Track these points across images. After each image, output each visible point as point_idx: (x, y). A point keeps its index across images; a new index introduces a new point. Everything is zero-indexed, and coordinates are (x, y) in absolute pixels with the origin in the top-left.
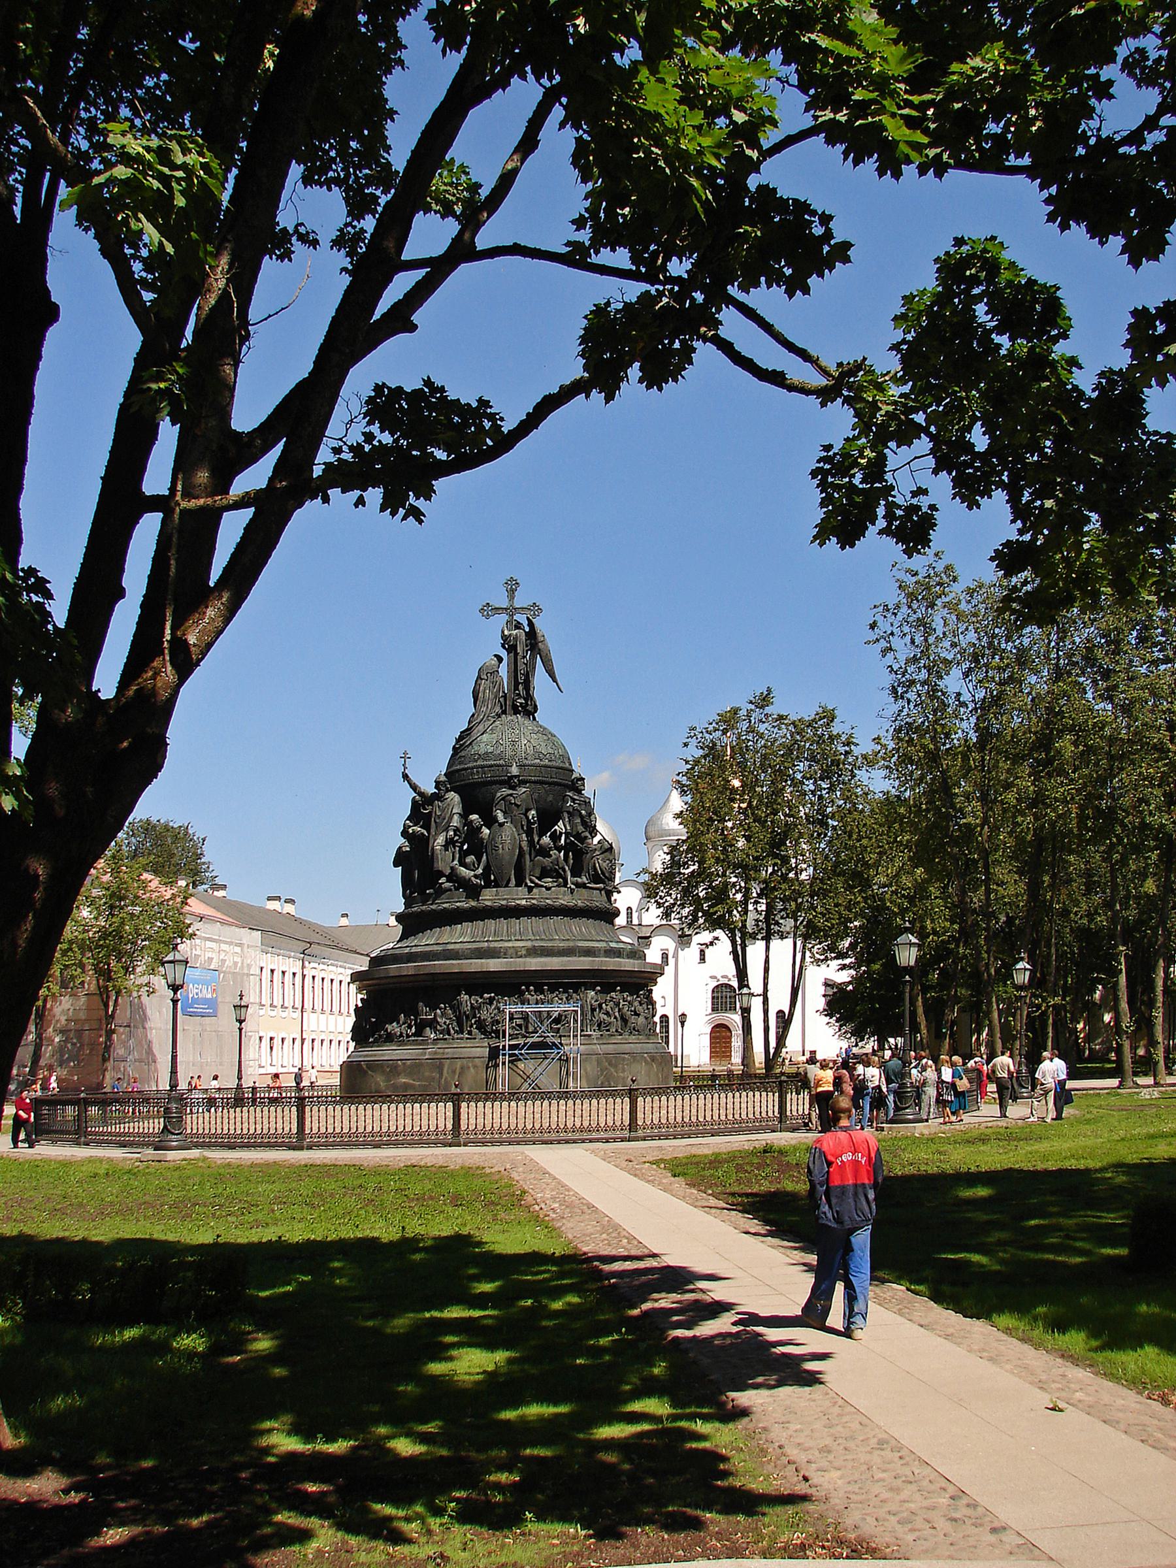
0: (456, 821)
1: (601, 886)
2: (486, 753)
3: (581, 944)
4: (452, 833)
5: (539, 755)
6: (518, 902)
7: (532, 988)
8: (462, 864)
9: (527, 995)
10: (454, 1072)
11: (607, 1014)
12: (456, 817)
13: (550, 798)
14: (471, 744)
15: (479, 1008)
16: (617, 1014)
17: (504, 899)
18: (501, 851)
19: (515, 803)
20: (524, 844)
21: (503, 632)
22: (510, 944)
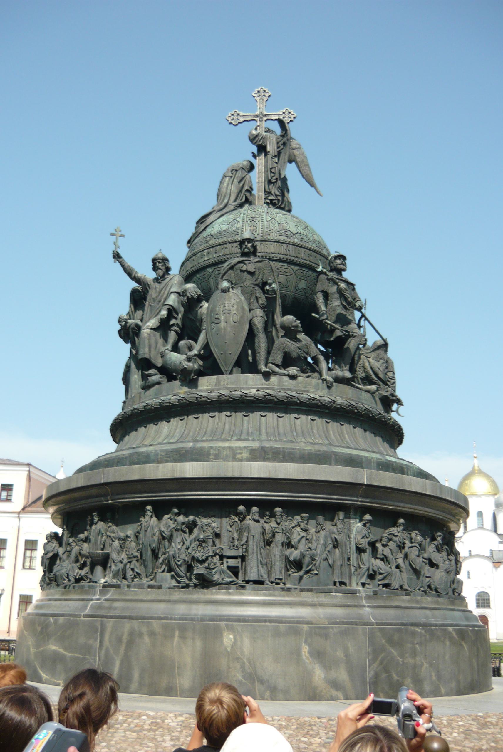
0: (172, 300)
1: (373, 387)
2: (220, 232)
3: (338, 450)
4: (164, 313)
5: (286, 232)
6: (245, 391)
7: (255, 509)
8: (175, 348)
9: (249, 521)
10: (119, 640)
11: (385, 559)
12: (173, 297)
13: (302, 284)
14: (204, 229)
15: (170, 539)
16: (400, 561)
17: (228, 389)
18: (222, 325)
19: (247, 271)
20: (259, 323)
21: (251, 133)
22: (227, 444)
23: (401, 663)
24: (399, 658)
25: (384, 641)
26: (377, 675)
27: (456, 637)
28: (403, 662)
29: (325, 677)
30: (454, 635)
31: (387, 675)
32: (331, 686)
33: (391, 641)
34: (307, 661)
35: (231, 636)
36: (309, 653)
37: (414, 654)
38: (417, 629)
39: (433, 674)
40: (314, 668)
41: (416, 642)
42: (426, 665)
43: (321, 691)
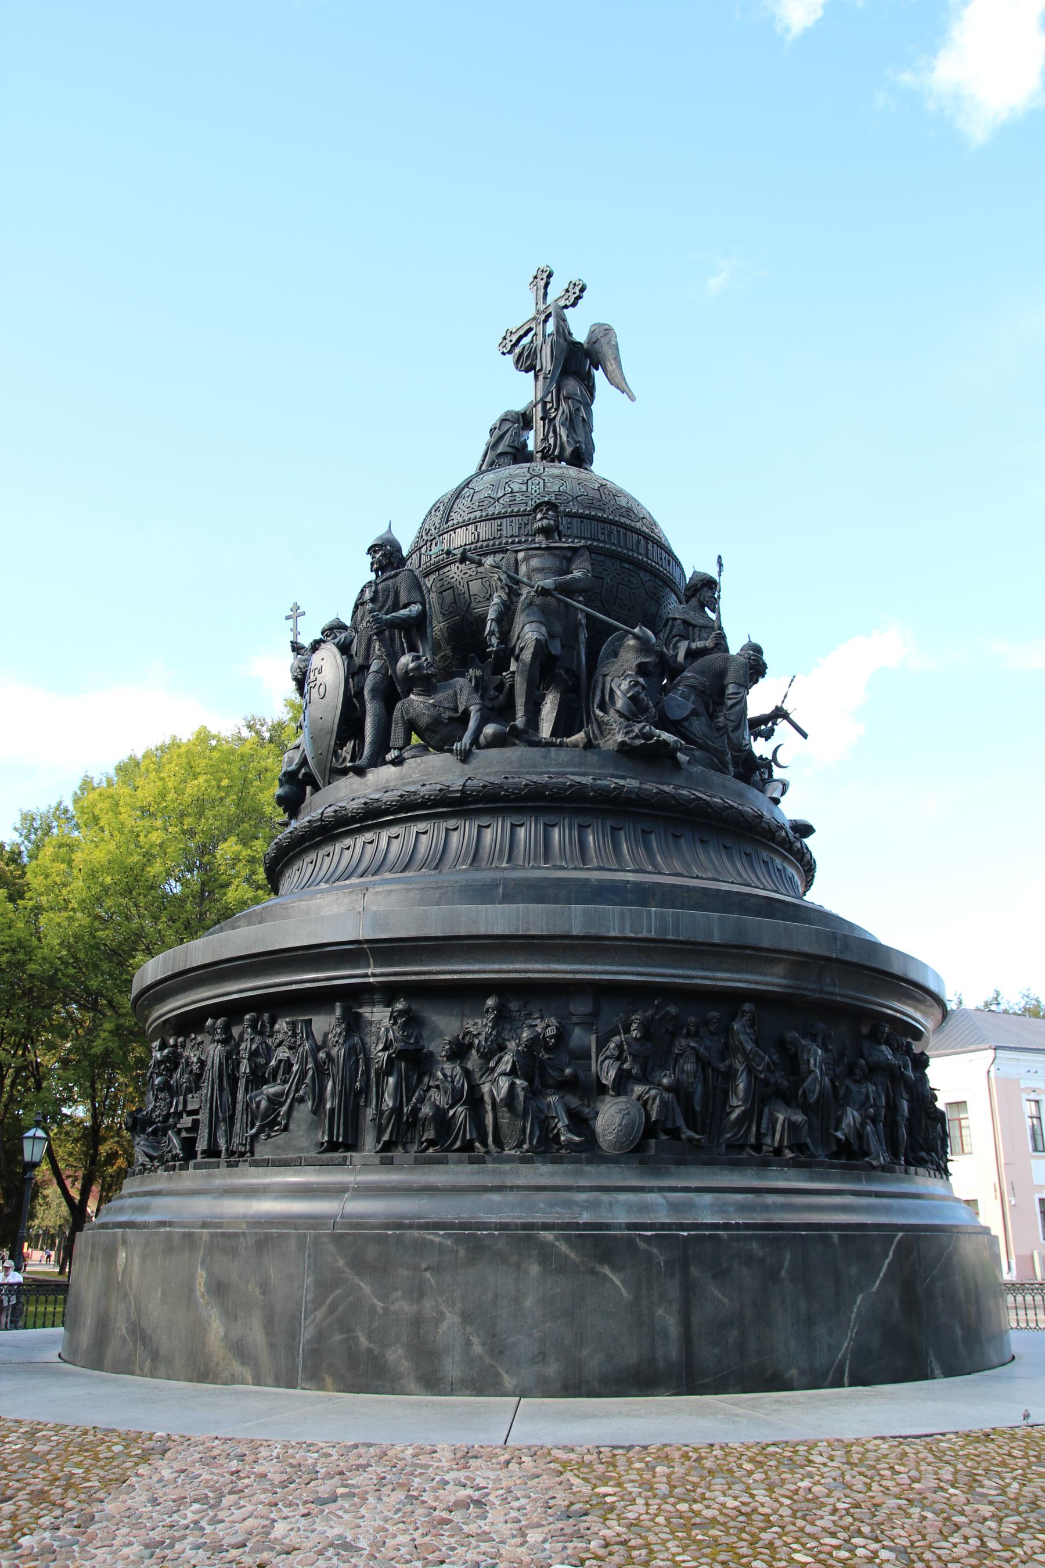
23: (381, 1312)
24: (375, 1300)
25: (341, 1263)
26: (320, 1336)
27: (573, 1255)
28: (386, 1310)
29: (226, 1335)
30: (563, 1247)
31: (344, 1336)
32: (234, 1355)
33: (358, 1264)
34: (201, 1300)
35: (124, 1255)
36: (205, 1284)
37: (418, 1292)
38: (430, 1237)
39: (475, 1340)
40: (210, 1316)
41: (424, 1266)
42: (452, 1318)
43: (218, 1364)
